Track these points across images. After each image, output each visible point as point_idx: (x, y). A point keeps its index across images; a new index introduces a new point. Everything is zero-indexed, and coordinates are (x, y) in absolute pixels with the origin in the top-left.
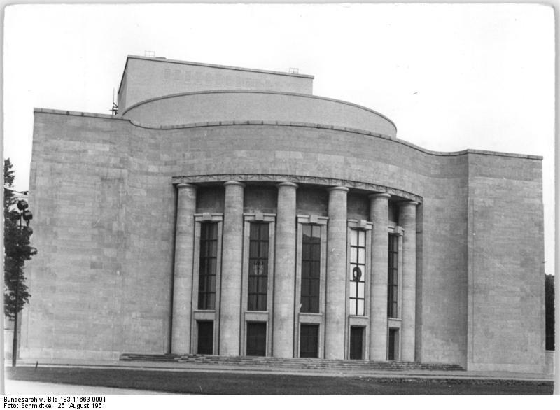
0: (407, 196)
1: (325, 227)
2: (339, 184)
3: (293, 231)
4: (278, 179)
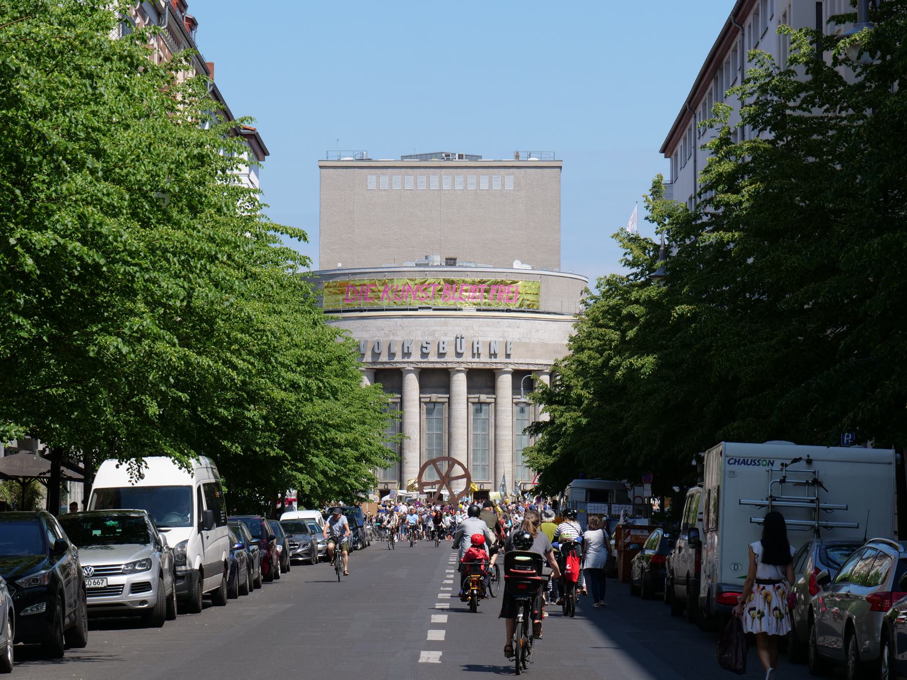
3: (416, 409)
4: (399, 366)
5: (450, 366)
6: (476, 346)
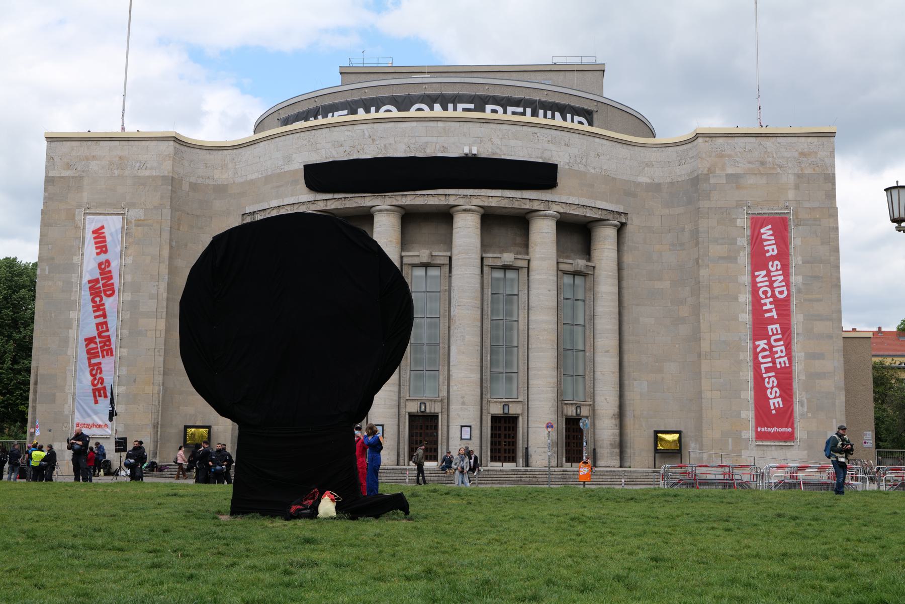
0: (590, 214)
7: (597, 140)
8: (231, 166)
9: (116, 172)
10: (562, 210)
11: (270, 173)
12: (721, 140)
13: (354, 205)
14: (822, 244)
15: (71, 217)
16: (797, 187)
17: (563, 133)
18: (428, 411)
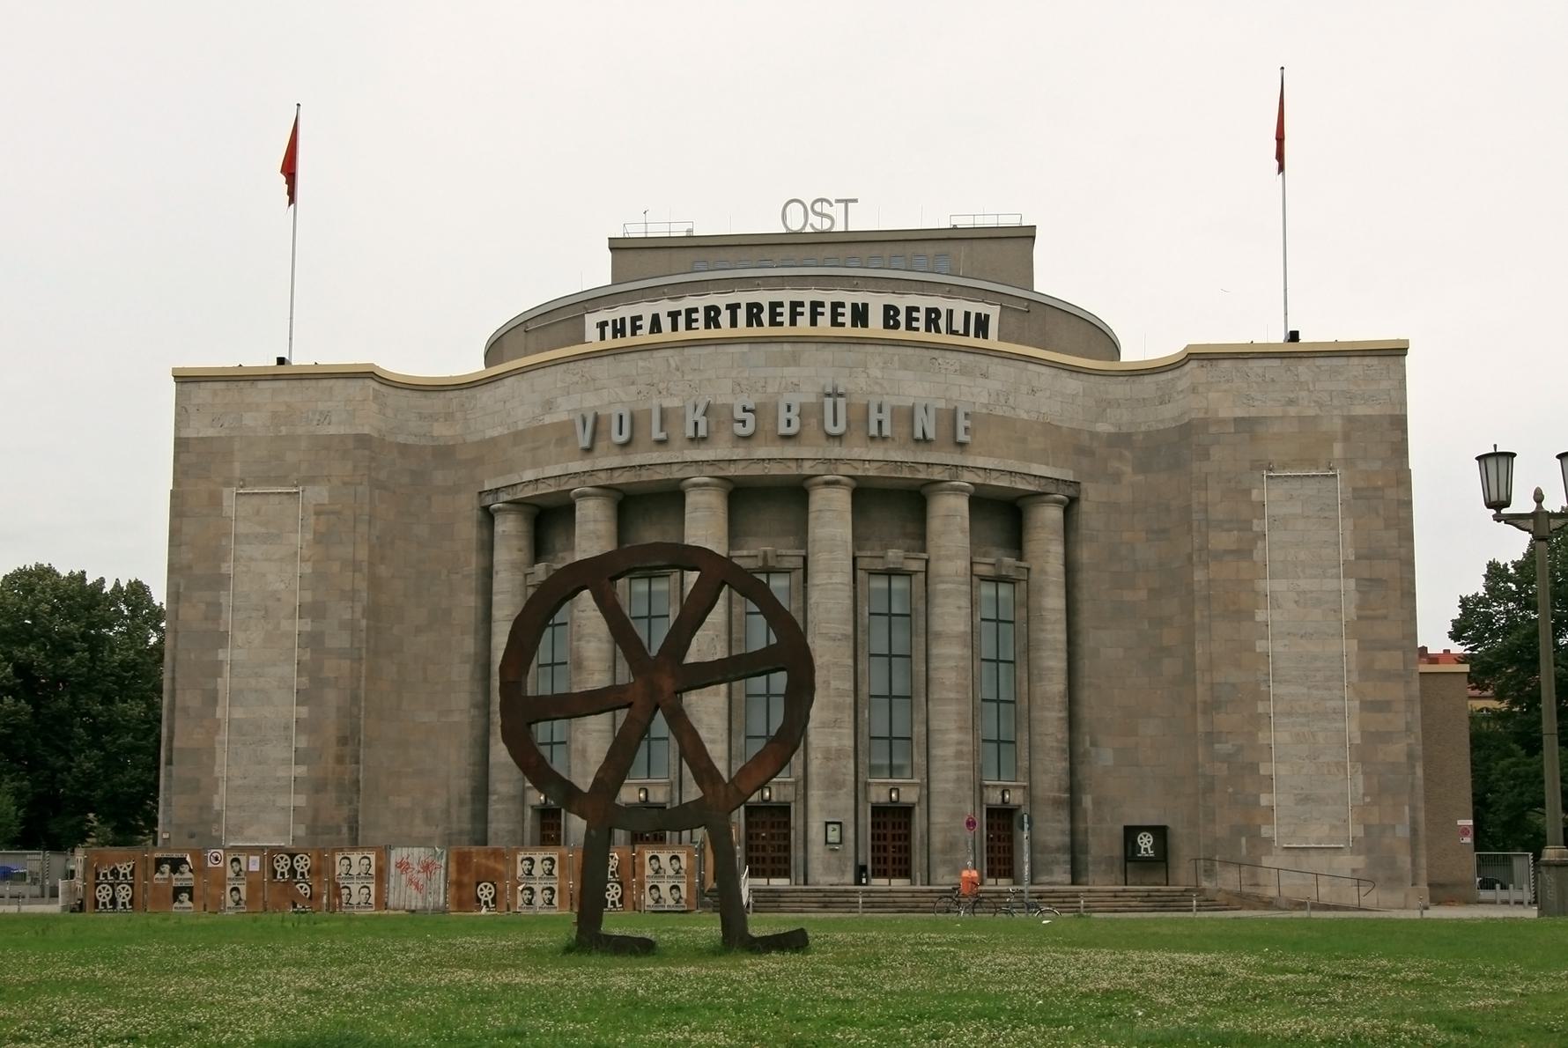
0: (1021, 485)
1: (922, 576)
2: (821, 469)
4: (677, 474)
5: (807, 469)
6: (874, 417)
7: (1031, 366)
8: (458, 415)
9: (283, 429)
10: (978, 481)
11: (521, 427)
12: (1226, 364)
13: (657, 477)
14: (1387, 527)
15: (215, 501)
16: (1347, 438)
17: (978, 357)
18: (774, 799)
